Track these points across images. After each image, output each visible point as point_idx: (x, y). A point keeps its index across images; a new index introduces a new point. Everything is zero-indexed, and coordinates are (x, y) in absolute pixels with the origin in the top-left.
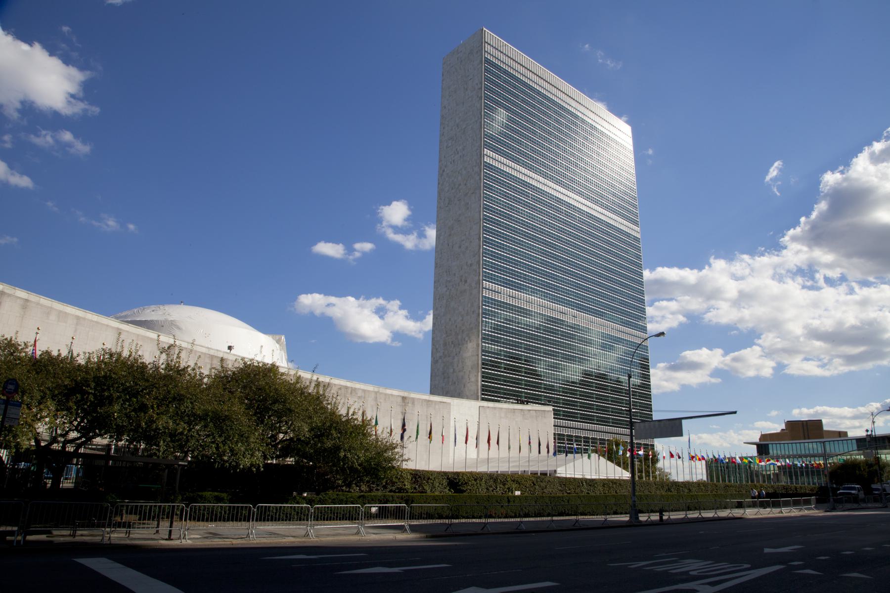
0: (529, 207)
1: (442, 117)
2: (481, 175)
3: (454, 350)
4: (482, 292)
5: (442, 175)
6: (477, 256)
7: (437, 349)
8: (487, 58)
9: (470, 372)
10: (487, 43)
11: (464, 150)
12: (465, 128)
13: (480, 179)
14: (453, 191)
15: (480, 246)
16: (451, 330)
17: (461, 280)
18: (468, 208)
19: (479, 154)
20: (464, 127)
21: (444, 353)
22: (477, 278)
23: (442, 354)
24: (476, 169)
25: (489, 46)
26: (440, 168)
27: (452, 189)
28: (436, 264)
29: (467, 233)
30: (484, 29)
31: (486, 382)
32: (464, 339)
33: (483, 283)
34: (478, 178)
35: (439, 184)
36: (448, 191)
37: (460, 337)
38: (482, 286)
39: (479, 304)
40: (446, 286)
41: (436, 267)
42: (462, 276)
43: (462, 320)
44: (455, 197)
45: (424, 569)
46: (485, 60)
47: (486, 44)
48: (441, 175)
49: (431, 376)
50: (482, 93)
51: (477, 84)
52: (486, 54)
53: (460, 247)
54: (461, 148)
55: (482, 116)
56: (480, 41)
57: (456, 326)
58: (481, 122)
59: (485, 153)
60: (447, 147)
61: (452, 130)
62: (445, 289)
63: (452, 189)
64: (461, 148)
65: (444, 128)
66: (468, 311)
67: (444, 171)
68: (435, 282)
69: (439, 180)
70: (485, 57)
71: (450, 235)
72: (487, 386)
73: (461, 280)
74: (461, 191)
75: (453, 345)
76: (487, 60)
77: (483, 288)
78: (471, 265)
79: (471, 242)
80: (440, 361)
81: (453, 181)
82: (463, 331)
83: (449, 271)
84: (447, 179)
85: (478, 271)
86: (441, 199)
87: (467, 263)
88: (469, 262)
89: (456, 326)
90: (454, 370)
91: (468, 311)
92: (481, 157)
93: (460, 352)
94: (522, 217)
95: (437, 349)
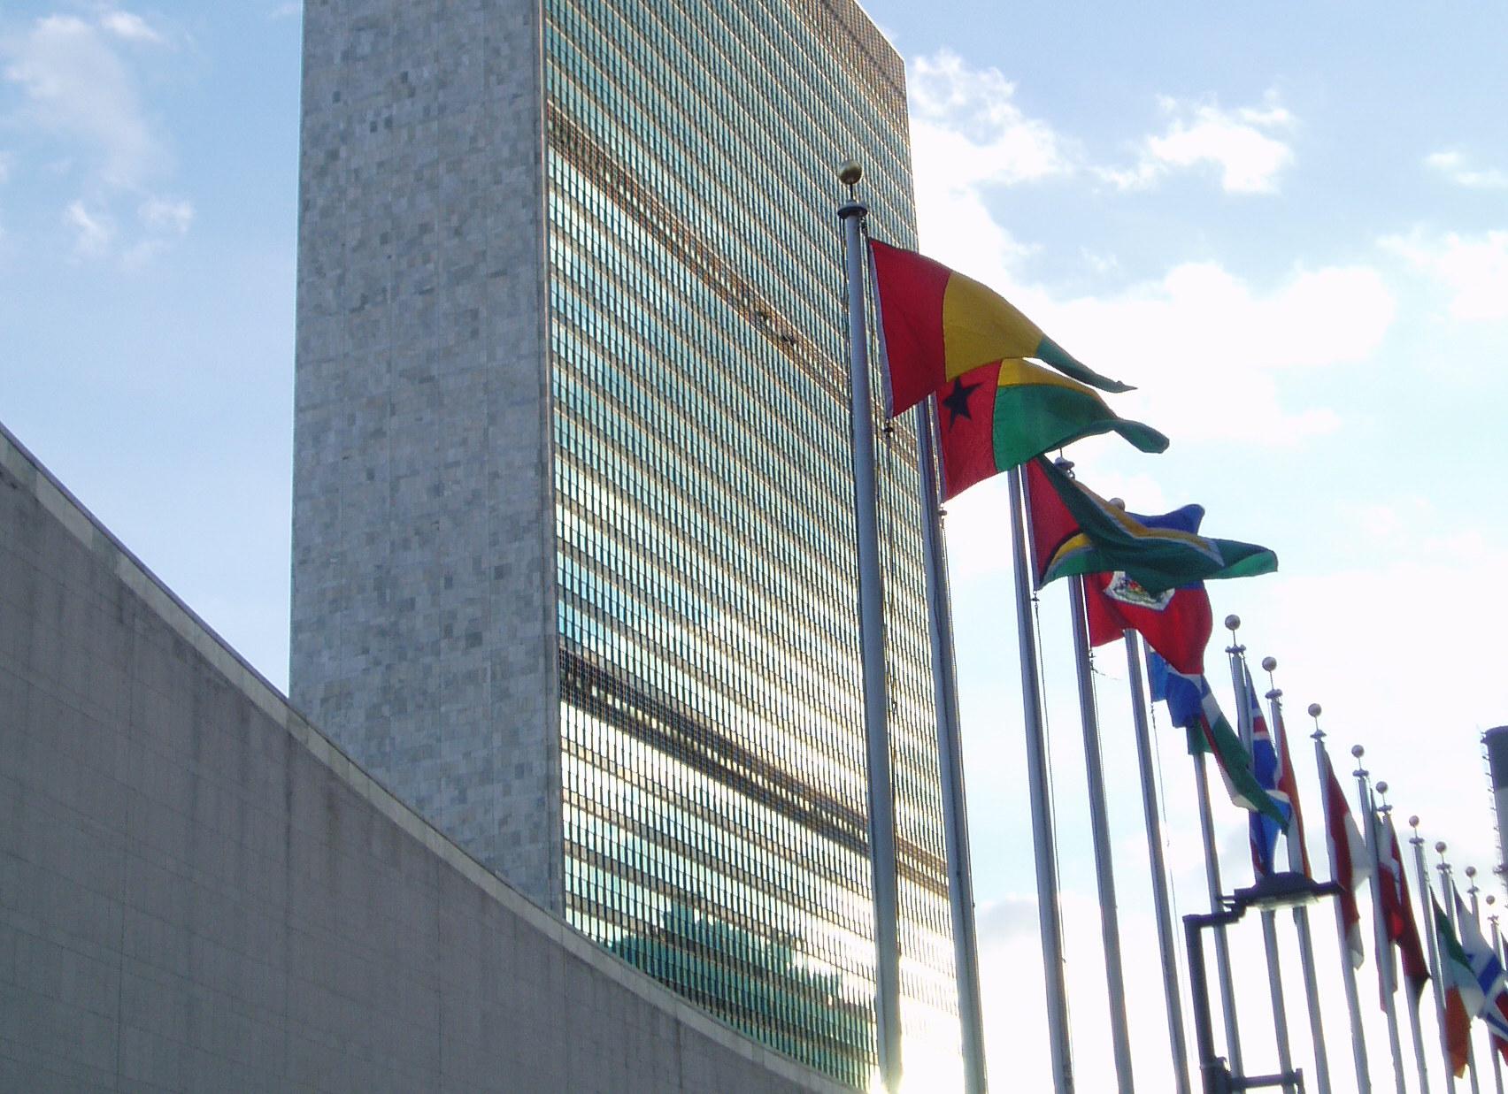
5: (322, 172)
14: (388, 249)
17: (448, 631)
27: (385, 240)
36: (362, 244)
43: (462, 799)
53: (437, 490)
62: (361, 662)
63: (385, 240)
67: (333, 155)
71: (379, 433)
74: (434, 254)
78: (500, 573)
79: (496, 475)
84: (353, 193)
86: (319, 272)
87: (477, 562)
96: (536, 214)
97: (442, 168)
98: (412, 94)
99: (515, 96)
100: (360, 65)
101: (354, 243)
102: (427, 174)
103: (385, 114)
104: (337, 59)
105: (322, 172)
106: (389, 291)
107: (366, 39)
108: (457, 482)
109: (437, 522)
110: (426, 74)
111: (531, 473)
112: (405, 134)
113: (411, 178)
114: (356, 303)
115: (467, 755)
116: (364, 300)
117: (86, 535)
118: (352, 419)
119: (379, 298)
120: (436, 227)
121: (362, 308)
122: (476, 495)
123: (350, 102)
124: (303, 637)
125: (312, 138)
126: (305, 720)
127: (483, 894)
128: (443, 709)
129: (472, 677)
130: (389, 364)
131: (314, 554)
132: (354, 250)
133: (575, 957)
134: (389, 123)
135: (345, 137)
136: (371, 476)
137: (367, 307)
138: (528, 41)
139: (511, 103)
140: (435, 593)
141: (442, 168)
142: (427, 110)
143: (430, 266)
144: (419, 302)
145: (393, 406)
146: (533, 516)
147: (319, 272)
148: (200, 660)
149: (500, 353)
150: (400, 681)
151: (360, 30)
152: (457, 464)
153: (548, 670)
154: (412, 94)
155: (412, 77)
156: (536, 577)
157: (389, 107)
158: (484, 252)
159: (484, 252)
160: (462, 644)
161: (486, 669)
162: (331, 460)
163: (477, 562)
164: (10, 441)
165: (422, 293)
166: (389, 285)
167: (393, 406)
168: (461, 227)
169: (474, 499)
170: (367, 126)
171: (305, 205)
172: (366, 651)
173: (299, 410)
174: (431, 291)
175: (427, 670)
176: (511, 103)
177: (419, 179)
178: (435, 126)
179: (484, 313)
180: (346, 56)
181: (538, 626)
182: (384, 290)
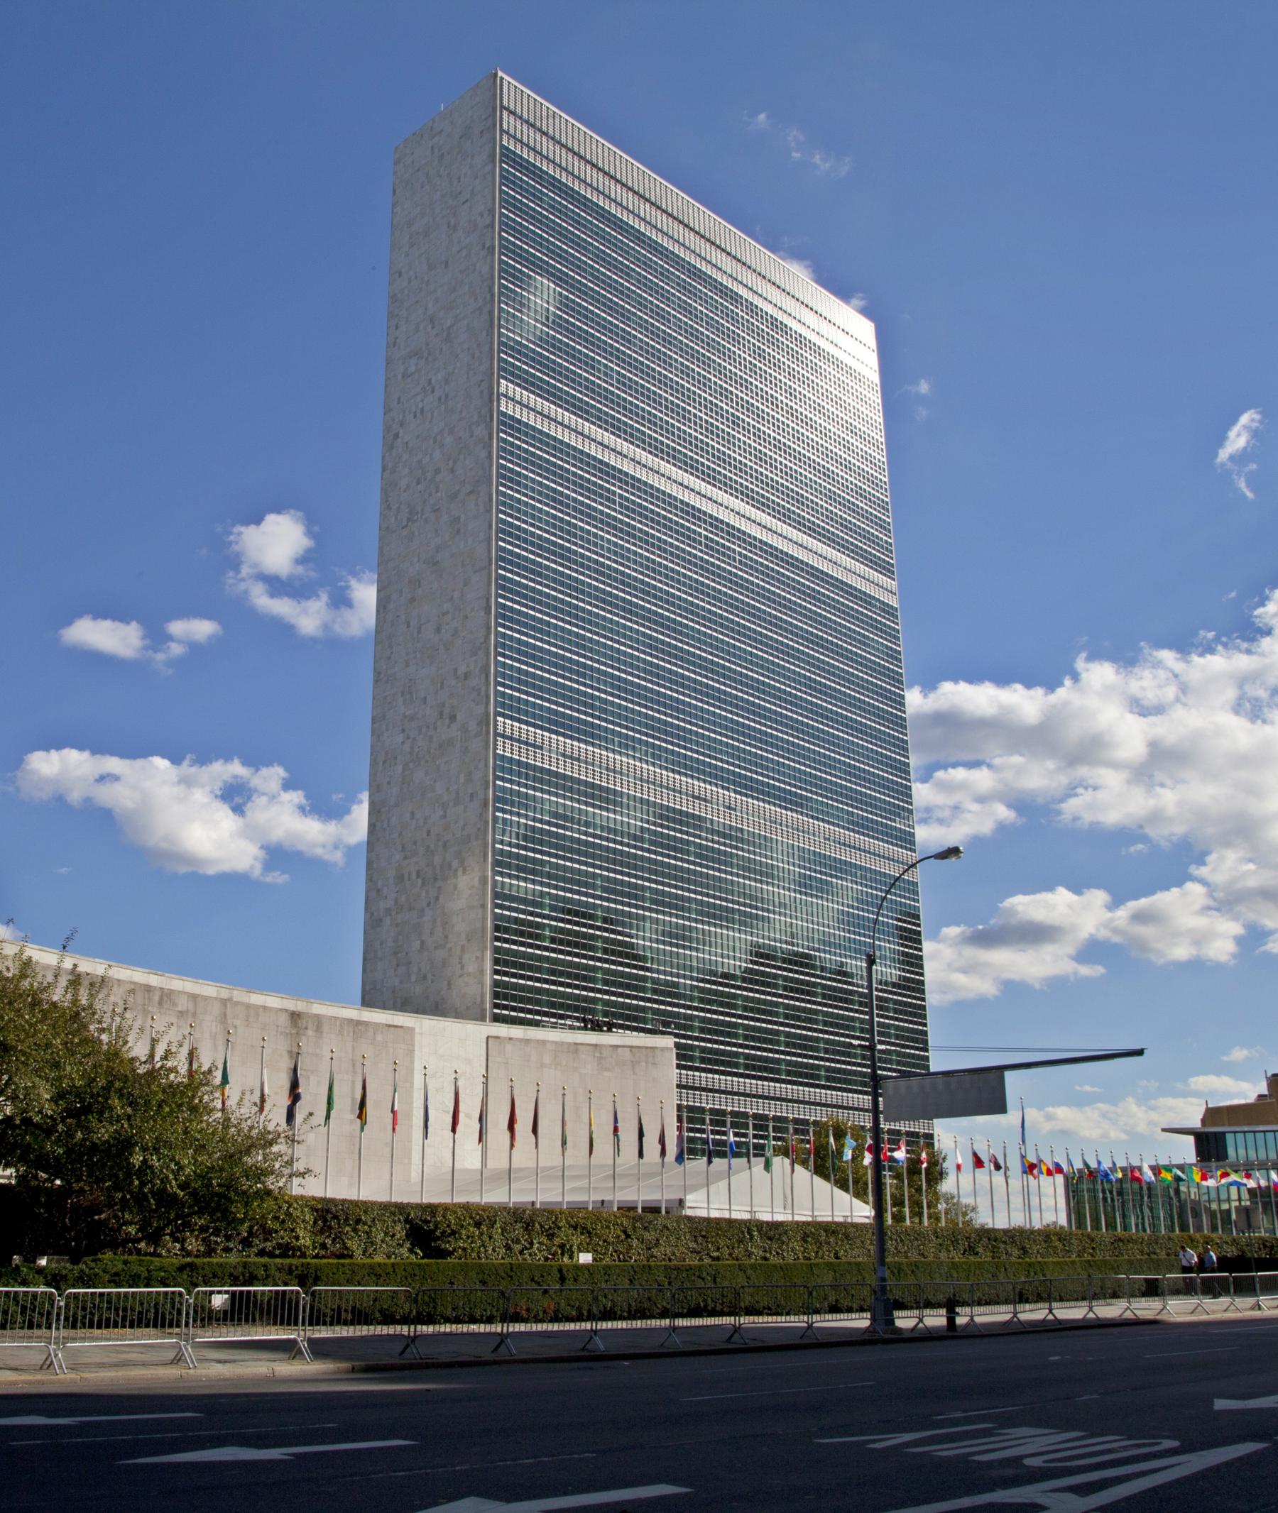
0: (615, 528)
1: (393, 298)
2: (491, 446)
3: (423, 894)
4: (495, 745)
5: (392, 447)
6: (481, 653)
7: (378, 891)
8: (507, 149)
9: (463, 946)
10: (507, 109)
11: (447, 381)
12: (452, 326)
13: (490, 456)
15: (489, 628)
16: (415, 843)
17: (441, 714)
18: (458, 531)
19: (486, 392)
20: (449, 323)
21: (396, 901)
22: (480, 710)
23: (390, 903)
24: (480, 431)
25: (512, 118)
26: (388, 429)
27: (418, 482)
28: (377, 673)
29: (456, 595)
30: (500, 74)
31: (506, 974)
32: (450, 865)
33: (496, 721)
34: (483, 454)
35: (384, 469)
36: (408, 486)
37: (437, 860)
38: (495, 729)
39: (487, 775)
40: (403, 731)
41: (376, 682)
42: (443, 705)
43: (445, 816)
44: (425, 502)
45: (346, 1451)
46: (502, 154)
47: (505, 114)
48: (389, 447)
49: (365, 959)
50: (493, 238)
51: (481, 215)
52: (505, 138)
53: (438, 630)
54: (439, 376)
55: (493, 295)
56: (491, 104)
57: (429, 833)
58: (491, 313)
59: (502, 390)
60: (406, 375)
62: (400, 738)
64: (439, 376)
65: (397, 328)
66: (457, 793)
67: (396, 436)
68: (374, 720)
69: (383, 458)
70: (502, 146)
71: (413, 600)
72: (507, 985)
73: (441, 714)
75: (420, 881)
76: (508, 155)
77: (496, 734)
78: (466, 676)
79: (466, 617)
80: (387, 921)
81: (420, 461)
82: (445, 846)
83: (411, 693)
84: (405, 457)
85: (483, 693)
86: (389, 507)
87: (456, 670)
88: (462, 670)
89: (429, 833)
90: (422, 943)
91: (457, 793)
92: (491, 401)
93: (437, 898)
94: (596, 553)
95: (378, 891)
98: (433, 391)
104: (400, 377)
107: (413, 361)
111: (483, 613)
116: (409, 520)
118: (401, 592)
122: (456, 630)
124: (376, 725)
129: (450, 742)
134: (422, 409)
136: (408, 626)
140: (436, 693)
142: (440, 399)
152: (448, 612)
156: (483, 676)
160: (447, 721)
169: (455, 633)
170: (412, 416)
175: (431, 737)
177: (435, 442)
178: (443, 408)
181: (483, 707)
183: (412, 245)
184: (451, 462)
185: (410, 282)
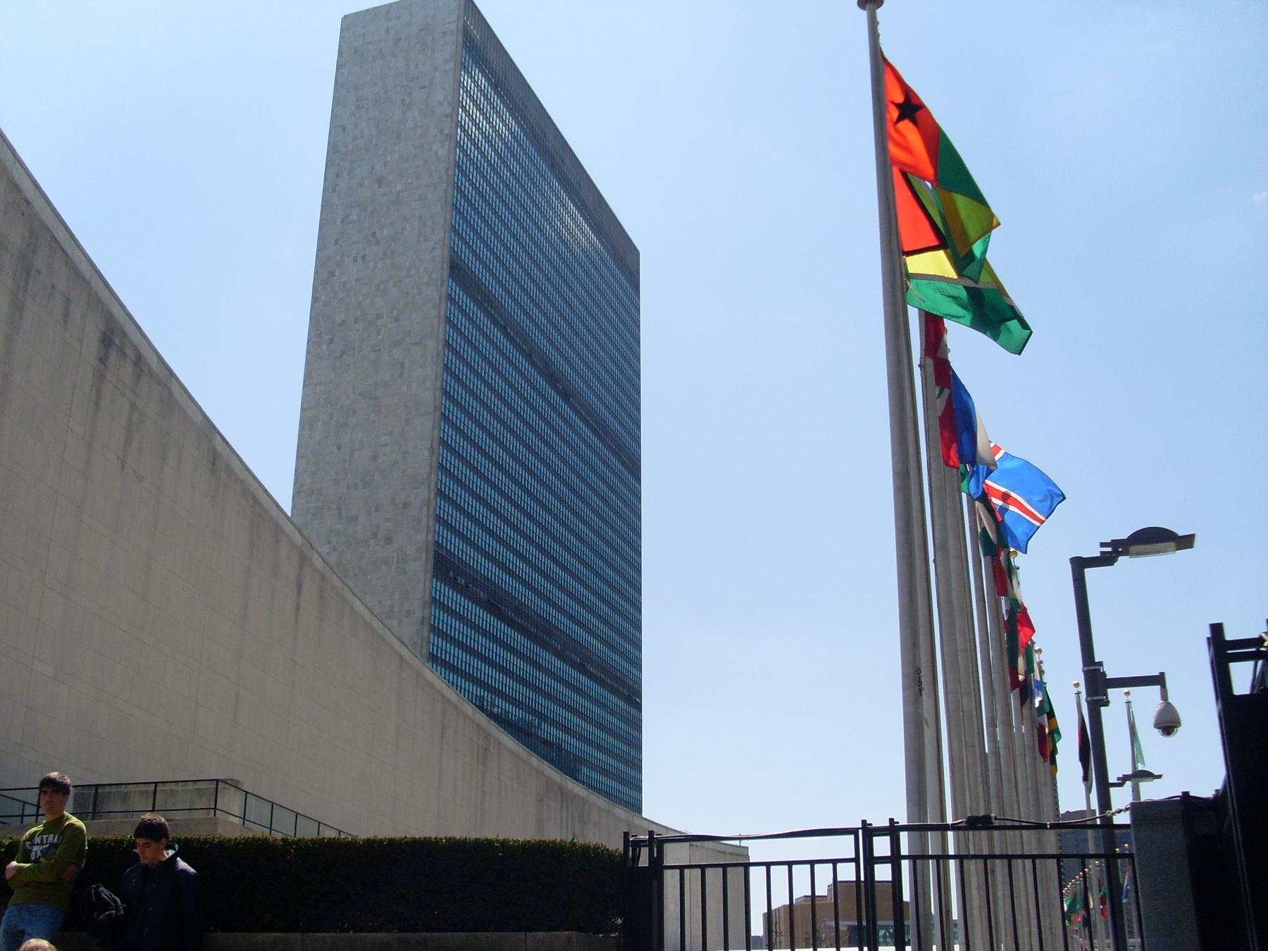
5: (325, 283)
12: (401, 191)
17: (375, 535)
18: (401, 375)
20: (399, 187)
27: (356, 320)
36: (344, 322)
53: (374, 458)
61: (361, 185)
63: (356, 320)
65: (337, 176)
67: (332, 273)
73: (375, 535)
78: (406, 505)
79: (407, 453)
96: (439, 313)
97: (390, 284)
99: (433, 249)
100: (351, 225)
101: (340, 322)
102: (382, 286)
103: (362, 254)
104: (338, 223)
105: (325, 283)
106: (357, 348)
108: (386, 455)
109: (374, 476)
110: (386, 233)
111: (426, 453)
112: (372, 265)
113: (373, 289)
114: (338, 355)
115: (380, 602)
116: (343, 352)
117: (198, 419)
118: (331, 417)
119: (351, 352)
120: (385, 317)
121: (341, 357)
123: (343, 246)
125: (321, 264)
126: (311, 546)
127: (401, 658)
128: (369, 577)
130: (354, 388)
131: (305, 488)
132: (339, 325)
133: (448, 701)
134: (364, 257)
135: (339, 264)
136: (339, 448)
137: (344, 356)
138: (443, 219)
139: (430, 252)
141: (390, 284)
142: (385, 253)
143: (380, 337)
144: (372, 356)
145: (354, 412)
146: (425, 476)
147: (319, 335)
148: (256, 500)
149: (414, 386)
150: (347, 560)
151: (352, 207)
153: (426, 560)
154: (377, 243)
155: (377, 235)
157: (364, 250)
158: (410, 331)
159: (410, 331)
161: (393, 557)
162: (318, 438)
163: (393, 500)
164: (159, 358)
165: (374, 351)
166: (357, 345)
167: (354, 412)
168: (398, 316)
171: (315, 299)
172: (329, 542)
173: (303, 409)
174: (379, 350)
176: (430, 252)
178: (388, 261)
179: (407, 363)
180: (343, 221)
181: (424, 536)
182: (354, 349)
183: (358, 108)
184: (395, 312)
185: (355, 138)
